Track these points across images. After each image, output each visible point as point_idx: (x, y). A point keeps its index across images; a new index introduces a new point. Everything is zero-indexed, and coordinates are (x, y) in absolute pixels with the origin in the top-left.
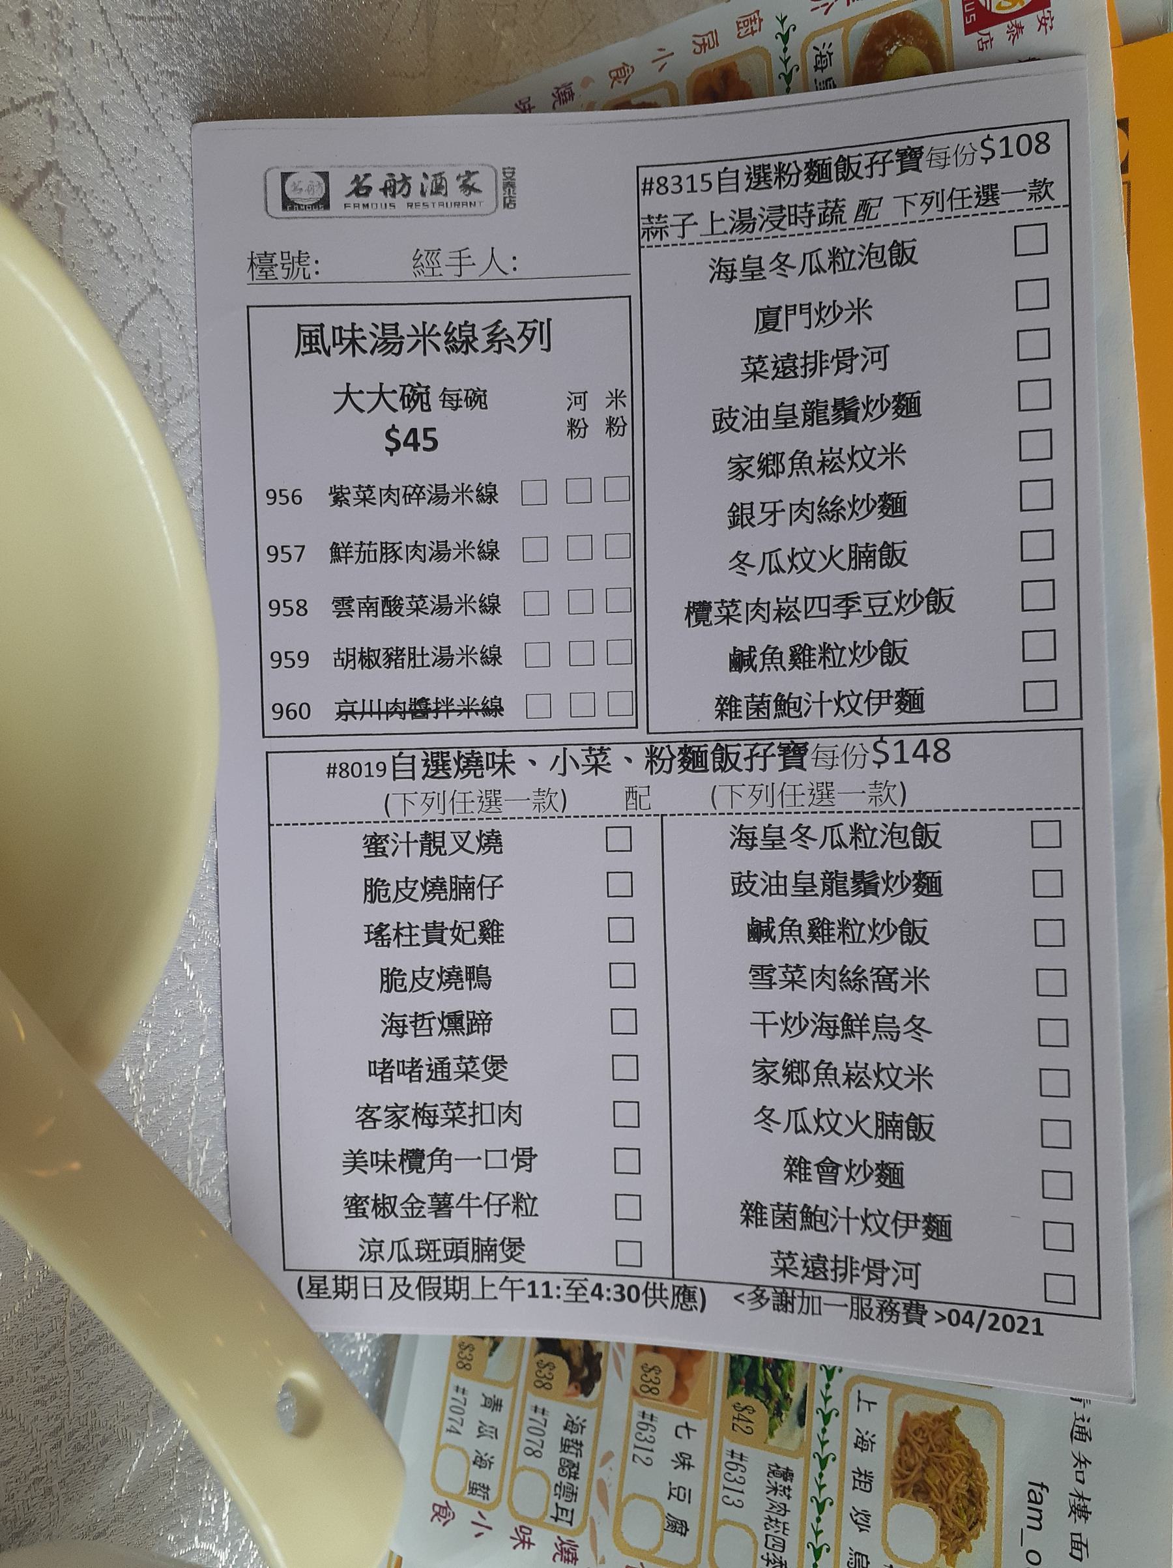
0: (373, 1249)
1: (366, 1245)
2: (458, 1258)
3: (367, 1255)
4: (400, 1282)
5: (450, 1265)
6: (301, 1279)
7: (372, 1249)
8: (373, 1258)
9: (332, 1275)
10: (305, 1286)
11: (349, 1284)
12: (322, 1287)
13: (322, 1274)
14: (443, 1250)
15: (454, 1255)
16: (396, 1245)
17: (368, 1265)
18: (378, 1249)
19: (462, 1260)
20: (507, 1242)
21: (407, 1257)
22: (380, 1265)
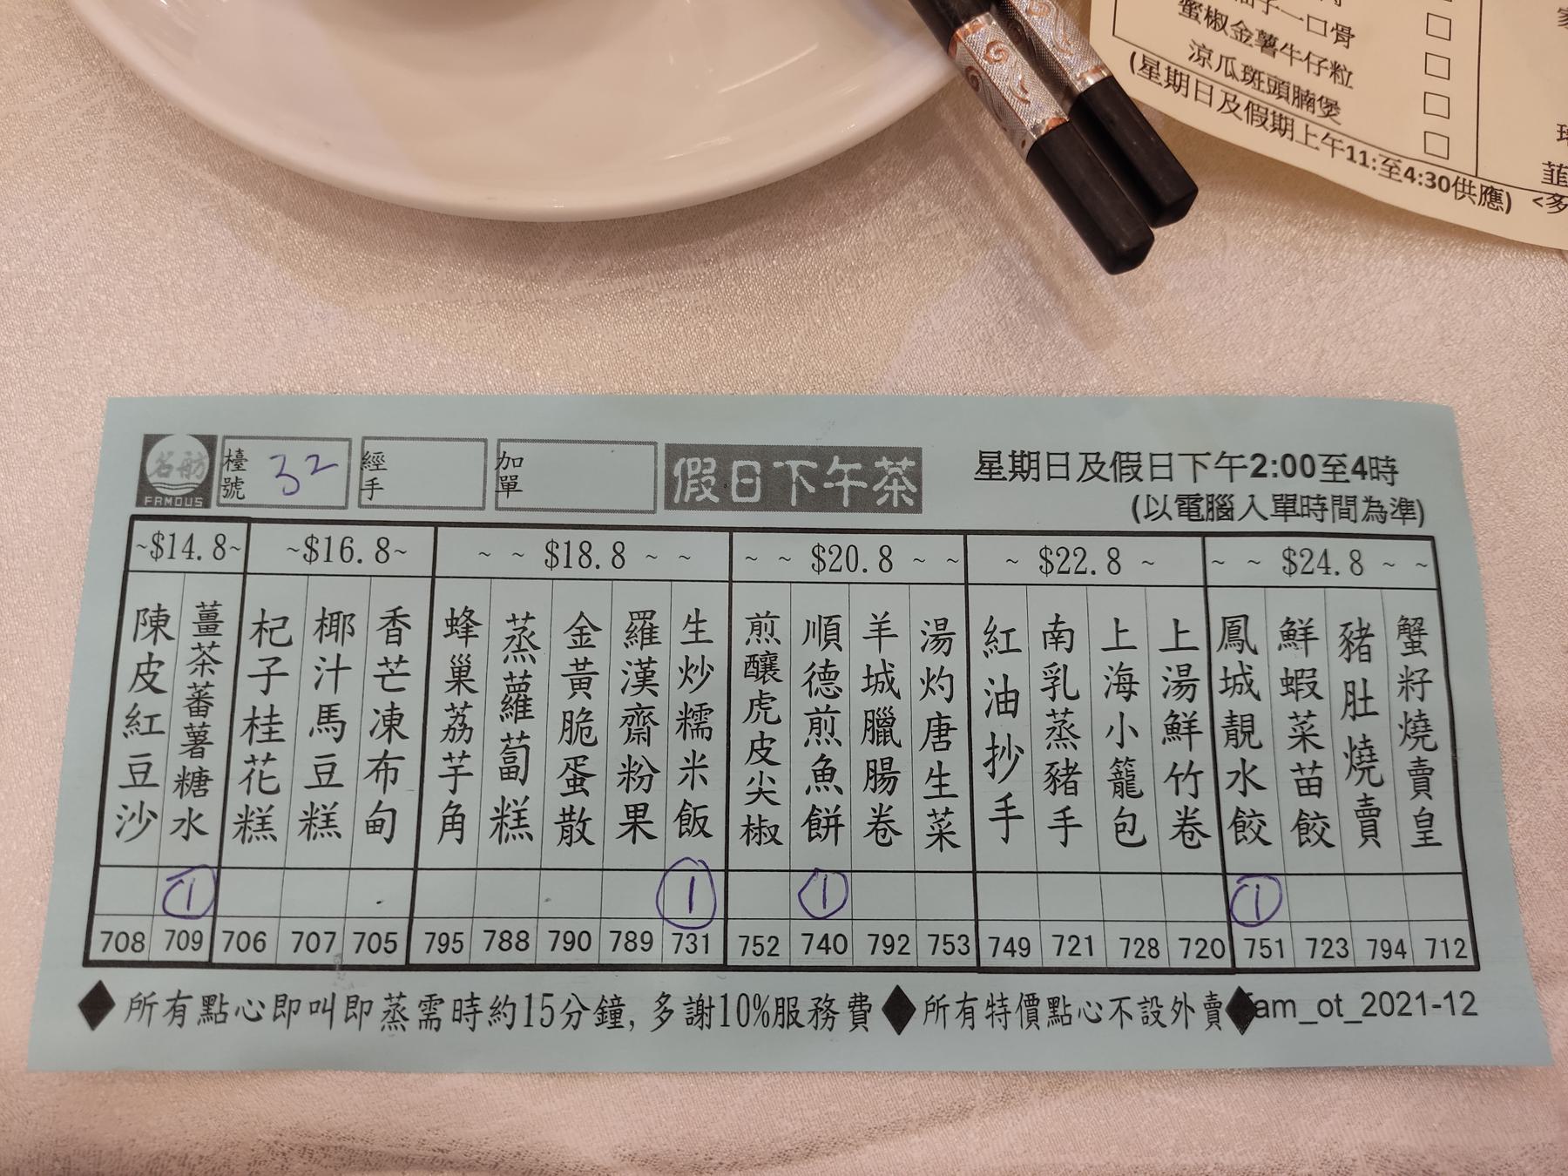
0: (1201, 53)
1: (1196, 48)
2: (1281, 97)
3: (1196, 57)
4: (1230, 98)
5: (1272, 99)
6: (1134, 54)
7: (1202, 54)
8: (1201, 62)
9: (1167, 64)
10: (1138, 63)
11: (1181, 80)
12: (1154, 70)
13: (1157, 59)
14: (1266, 81)
15: (1277, 91)
16: (1224, 60)
17: (1196, 66)
18: (1207, 56)
19: (1283, 99)
20: (1324, 100)
21: (1233, 75)
22: (1206, 70)
